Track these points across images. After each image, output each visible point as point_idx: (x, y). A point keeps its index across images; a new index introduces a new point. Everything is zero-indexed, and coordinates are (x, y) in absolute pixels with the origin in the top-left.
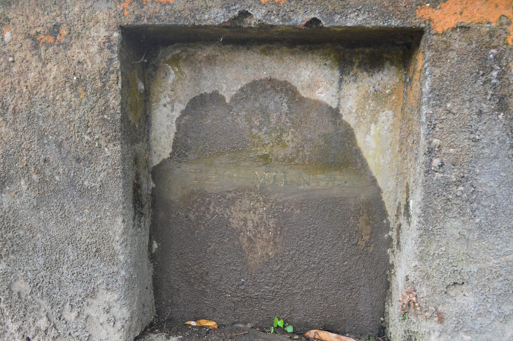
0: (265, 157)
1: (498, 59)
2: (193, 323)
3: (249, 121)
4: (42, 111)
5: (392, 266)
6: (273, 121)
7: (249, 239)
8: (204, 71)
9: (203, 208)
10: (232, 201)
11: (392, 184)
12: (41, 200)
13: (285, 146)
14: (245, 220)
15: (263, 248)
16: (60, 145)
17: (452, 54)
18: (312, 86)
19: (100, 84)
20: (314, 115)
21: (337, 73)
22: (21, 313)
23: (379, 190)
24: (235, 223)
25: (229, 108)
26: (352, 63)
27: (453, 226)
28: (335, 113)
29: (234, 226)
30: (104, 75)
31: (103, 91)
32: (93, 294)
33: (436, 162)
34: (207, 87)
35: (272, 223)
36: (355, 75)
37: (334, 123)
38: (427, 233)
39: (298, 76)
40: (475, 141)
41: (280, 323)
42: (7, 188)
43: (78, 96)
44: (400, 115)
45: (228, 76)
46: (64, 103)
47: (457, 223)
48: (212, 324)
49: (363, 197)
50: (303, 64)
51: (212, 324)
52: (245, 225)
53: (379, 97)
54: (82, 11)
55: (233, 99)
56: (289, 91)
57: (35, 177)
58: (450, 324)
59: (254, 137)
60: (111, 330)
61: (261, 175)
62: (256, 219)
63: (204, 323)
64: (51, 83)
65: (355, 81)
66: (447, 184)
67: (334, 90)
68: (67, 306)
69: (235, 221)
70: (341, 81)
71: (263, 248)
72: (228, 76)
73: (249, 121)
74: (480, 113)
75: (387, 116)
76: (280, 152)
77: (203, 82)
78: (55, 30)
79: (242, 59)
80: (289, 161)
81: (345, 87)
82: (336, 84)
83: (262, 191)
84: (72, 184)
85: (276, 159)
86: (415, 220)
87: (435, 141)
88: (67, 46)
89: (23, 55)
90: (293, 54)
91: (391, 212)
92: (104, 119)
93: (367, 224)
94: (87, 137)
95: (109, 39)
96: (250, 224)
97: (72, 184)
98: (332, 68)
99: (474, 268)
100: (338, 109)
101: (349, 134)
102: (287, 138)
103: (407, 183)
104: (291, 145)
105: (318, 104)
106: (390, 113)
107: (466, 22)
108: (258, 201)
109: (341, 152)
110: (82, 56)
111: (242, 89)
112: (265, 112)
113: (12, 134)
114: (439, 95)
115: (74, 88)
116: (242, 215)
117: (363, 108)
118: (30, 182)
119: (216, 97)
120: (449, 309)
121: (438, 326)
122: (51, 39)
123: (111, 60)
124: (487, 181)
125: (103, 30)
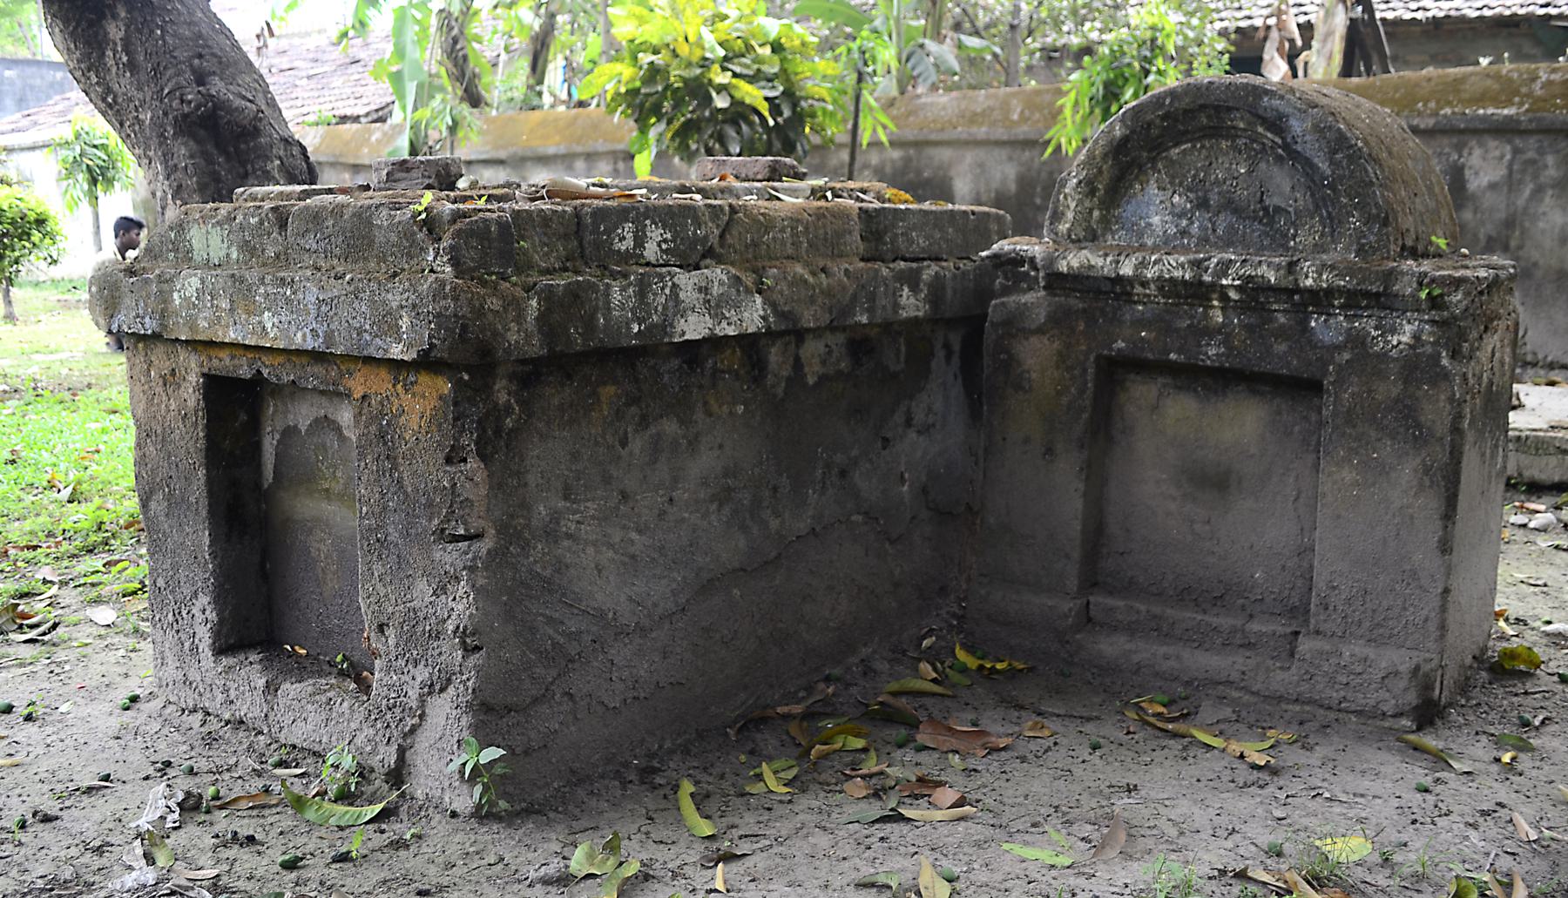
0: (327, 490)
48: (303, 652)
51: (303, 652)
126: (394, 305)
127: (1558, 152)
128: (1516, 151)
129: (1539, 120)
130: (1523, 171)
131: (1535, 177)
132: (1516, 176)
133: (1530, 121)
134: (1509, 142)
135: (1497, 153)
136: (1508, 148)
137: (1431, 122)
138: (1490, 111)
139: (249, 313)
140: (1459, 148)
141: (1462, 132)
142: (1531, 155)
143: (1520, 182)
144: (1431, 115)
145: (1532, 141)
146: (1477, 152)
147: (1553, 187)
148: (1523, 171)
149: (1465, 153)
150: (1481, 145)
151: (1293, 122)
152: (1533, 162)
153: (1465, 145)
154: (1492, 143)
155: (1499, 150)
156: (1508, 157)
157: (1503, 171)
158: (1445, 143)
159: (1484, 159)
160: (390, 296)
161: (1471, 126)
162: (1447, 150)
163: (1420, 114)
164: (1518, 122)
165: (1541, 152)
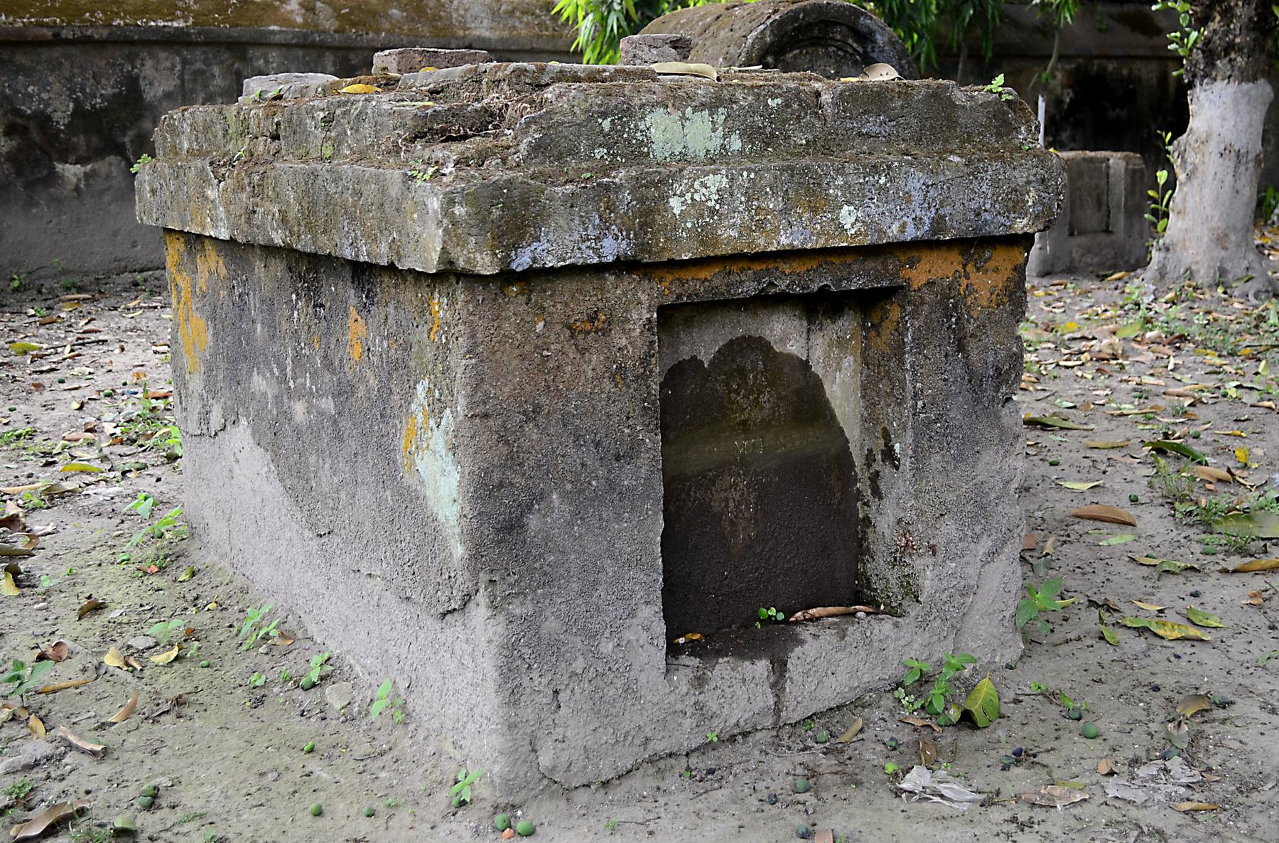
0: (744, 423)
1: (955, 306)
2: (681, 640)
3: (727, 384)
4: (576, 407)
5: (867, 521)
6: (751, 382)
7: (731, 521)
8: (682, 335)
9: (683, 496)
10: (713, 481)
11: (857, 432)
12: (577, 514)
13: (762, 408)
14: (726, 500)
15: (744, 529)
16: (598, 445)
17: (926, 307)
18: (783, 340)
19: (642, 370)
20: (786, 370)
21: (805, 324)
22: (554, 660)
23: (847, 441)
24: (717, 506)
25: (708, 373)
26: (817, 312)
27: (936, 460)
28: (806, 365)
29: (716, 510)
30: (645, 361)
31: (643, 378)
32: (632, 614)
33: (920, 403)
34: (685, 353)
35: (752, 498)
36: (821, 323)
37: (805, 376)
38: (918, 471)
39: (772, 330)
40: (945, 380)
41: (773, 611)
42: (536, 507)
43: (616, 386)
44: (859, 360)
45: (706, 338)
46: (604, 396)
47: (938, 457)
49: (833, 451)
50: (775, 317)
52: (727, 506)
53: (841, 343)
54: (625, 294)
55: (711, 363)
56: (762, 345)
57: (569, 487)
58: (940, 555)
59: (733, 403)
60: (652, 649)
61: (742, 445)
62: (737, 497)
63: (689, 636)
64: (590, 374)
65: (821, 330)
66: (929, 423)
67: (803, 341)
68: (607, 634)
69: (717, 504)
70: (808, 331)
71: (744, 529)
72: (706, 338)
73: (727, 384)
74: (946, 355)
75: (849, 362)
76: (758, 416)
77: (682, 348)
78: (592, 318)
79: (719, 318)
80: (766, 425)
81: (812, 337)
82: (804, 335)
83: (743, 463)
84: (611, 486)
85: (755, 424)
86: (906, 463)
87: (919, 385)
88: (606, 332)
89: (559, 347)
90: (765, 307)
91: (858, 461)
92: (644, 407)
93: (839, 479)
94: (627, 431)
95: (649, 320)
96: (731, 504)
97: (611, 486)
98: (801, 319)
99: (952, 497)
100: (807, 361)
101: (818, 385)
102: (764, 398)
103: (885, 429)
104: (768, 405)
105: (791, 357)
106: (851, 358)
107: (932, 277)
108: (739, 475)
109: (809, 404)
110: (624, 342)
111: (719, 351)
112: (742, 372)
113: (546, 439)
114: (919, 344)
115: (612, 378)
116: (723, 495)
117: (829, 357)
118: (564, 495)
119: (695, 362)
120: (939, 541)
121: (931, 560)
122: (588, 327)
123: (652, 343)
124: (955, 416)
125: (644, 311)
126: (1021, 181)
127: (222, 63)
128: (185, 62)
129: (206, 33)
130: (194, 81)
131: (205, 86)
132: (189, 86)
133: (199, 34)
134: (178, 54)
135: (168, 64)
136: (178, 59)
137: (105, 32)
138: (161, 24)
139: (815, 210)
140: (131, 59)
141: (132, 43)
142: (199, 65)
143: (193, 91)
144: (104, 26)
145: (198, 53)
146: (149, 63)
147: (221, 95)
148: (194, 81)
149: (138, 63)
150: (152, 56)
151: (878, 37)
152: (202, 72)
153: (137, 55)
154: (163, 55)
155: (166, 58)
156: (179, 67)
157: (177, 82)
158: (118, 55)
159: (157, 70)
160: (1016, 173)
161: (144, 37)
162: (120, 61)
163: (92, 25)
164: (189, 34)
165: (207, 62)
